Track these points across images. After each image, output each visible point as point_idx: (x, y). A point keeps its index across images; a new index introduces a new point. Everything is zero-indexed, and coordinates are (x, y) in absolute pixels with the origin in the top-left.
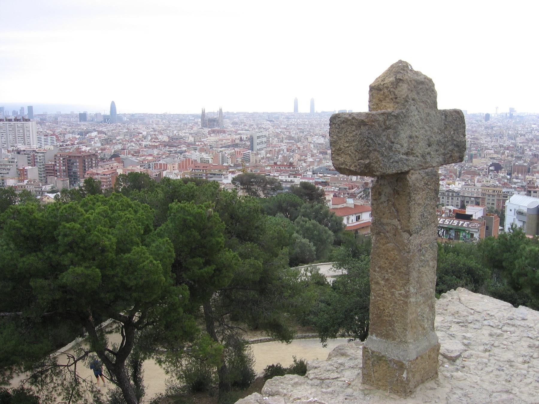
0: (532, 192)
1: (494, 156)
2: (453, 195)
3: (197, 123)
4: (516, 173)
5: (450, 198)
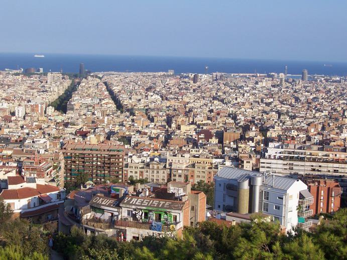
0: (245, 162)
2: (158, 168)
5: (155, 171)
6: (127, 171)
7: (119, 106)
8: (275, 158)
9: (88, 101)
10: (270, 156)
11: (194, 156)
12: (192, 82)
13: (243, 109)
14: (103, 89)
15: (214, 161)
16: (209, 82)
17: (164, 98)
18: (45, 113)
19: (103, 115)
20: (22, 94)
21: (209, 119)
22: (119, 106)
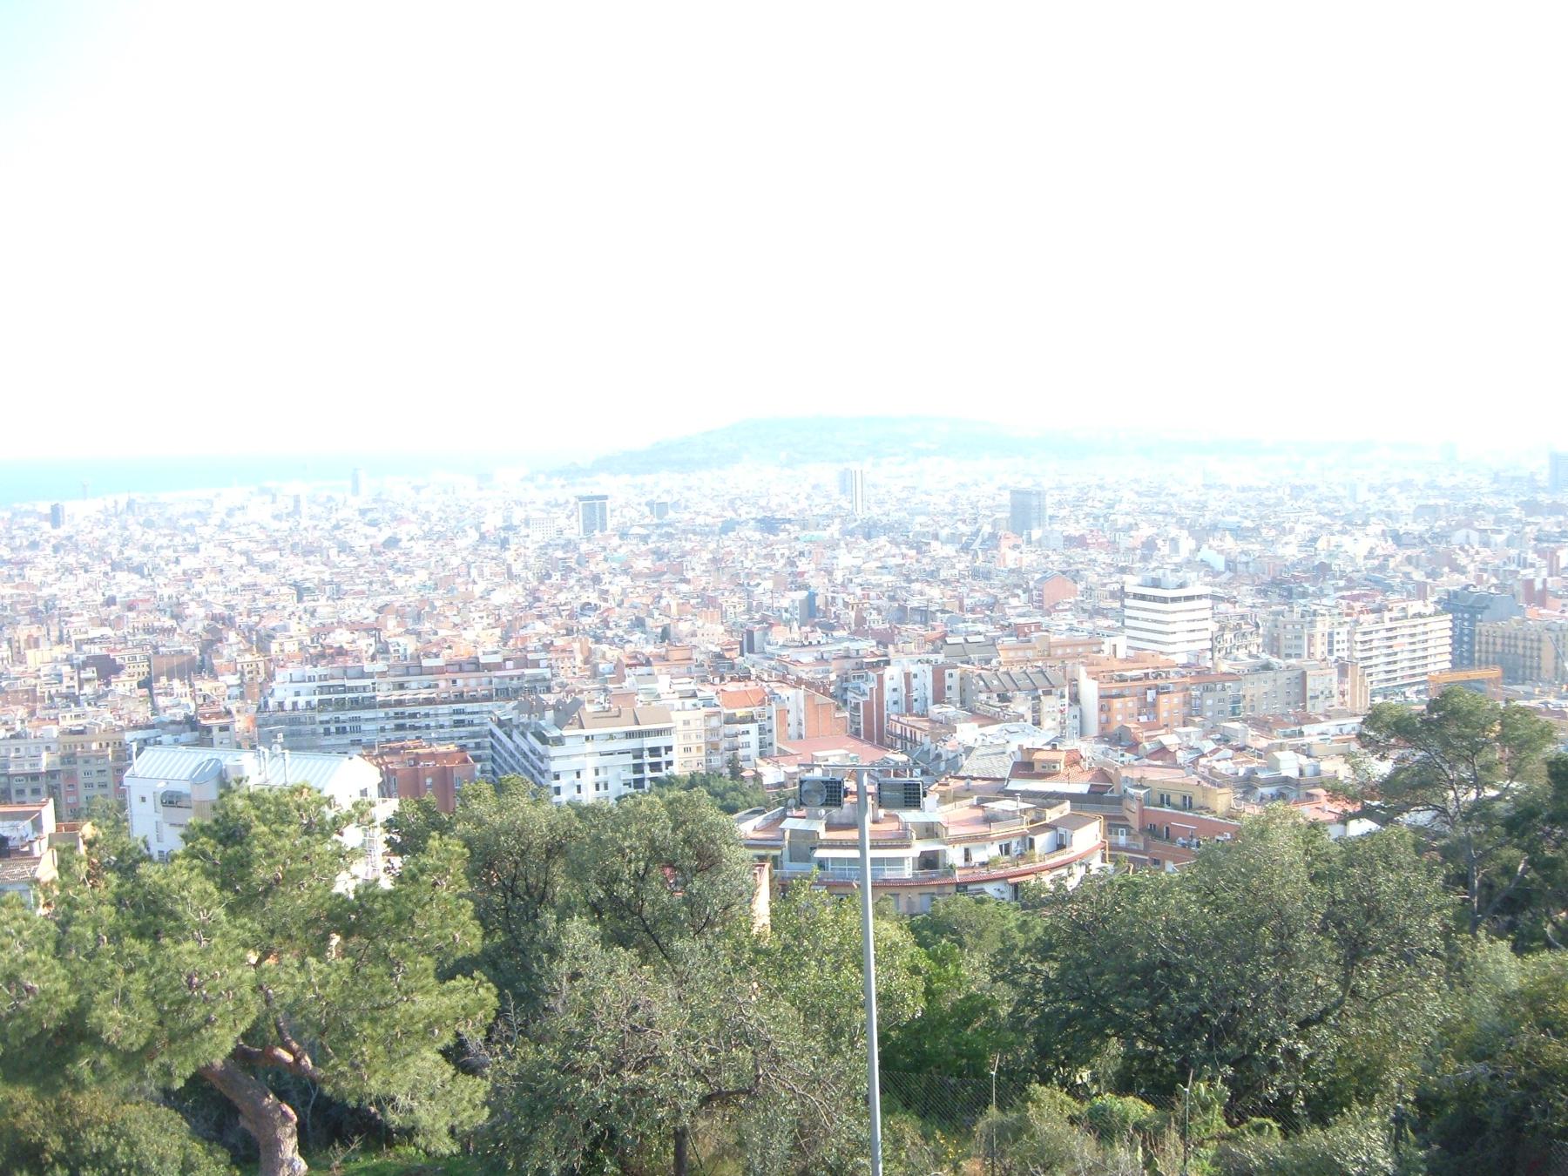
1: (95, 633)
4: (164, 679)
12: (46, 526)
13: (198, 588)
21: (103, 623)
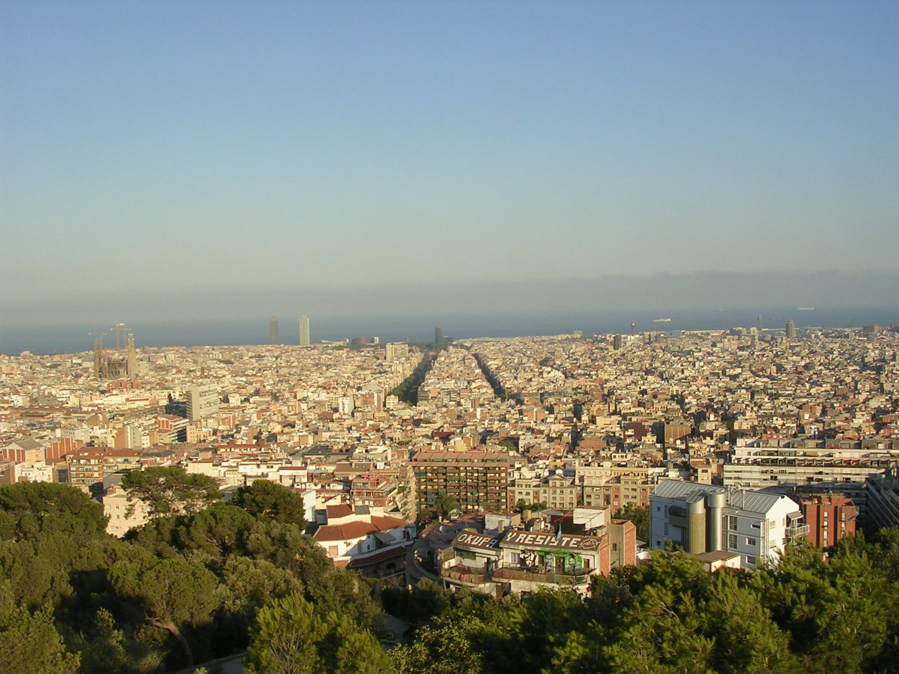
0: (700, 471)
1: (633, 410)
2: (562, 485)
3: (86, 370)
5: (558, 491)
6: (513, 492)
7: (499, 391)
8: (747, 464)
9: (451, 384)
10: (739, 460)
11: (619, 465)
12: (611, 348)
13: (694, 388)
14: (473, 365)
15: (651, 471)
16: (639, 347)
17: (568, 375)
18: (385, 405)
19: (474, 406)
20: (349, 378)
21: (641, 404)
22: (499, 391)
